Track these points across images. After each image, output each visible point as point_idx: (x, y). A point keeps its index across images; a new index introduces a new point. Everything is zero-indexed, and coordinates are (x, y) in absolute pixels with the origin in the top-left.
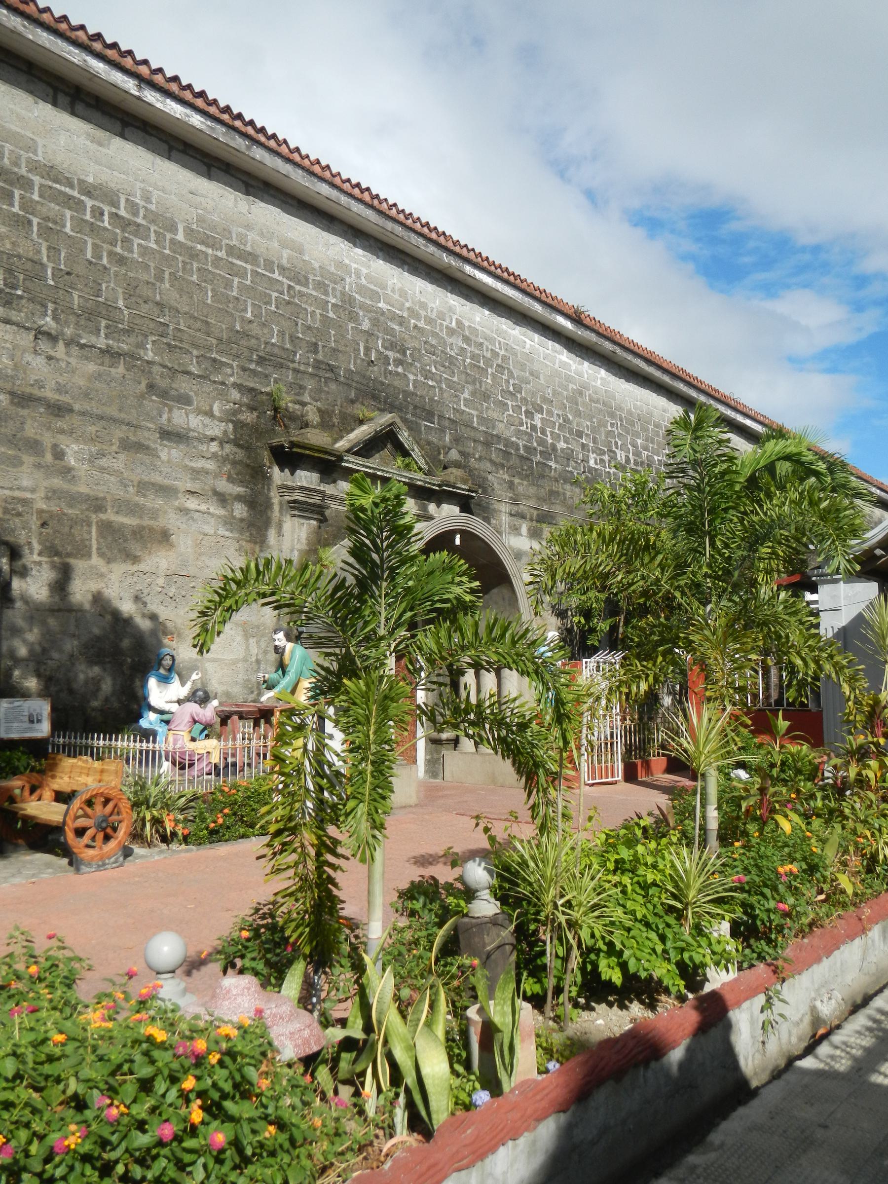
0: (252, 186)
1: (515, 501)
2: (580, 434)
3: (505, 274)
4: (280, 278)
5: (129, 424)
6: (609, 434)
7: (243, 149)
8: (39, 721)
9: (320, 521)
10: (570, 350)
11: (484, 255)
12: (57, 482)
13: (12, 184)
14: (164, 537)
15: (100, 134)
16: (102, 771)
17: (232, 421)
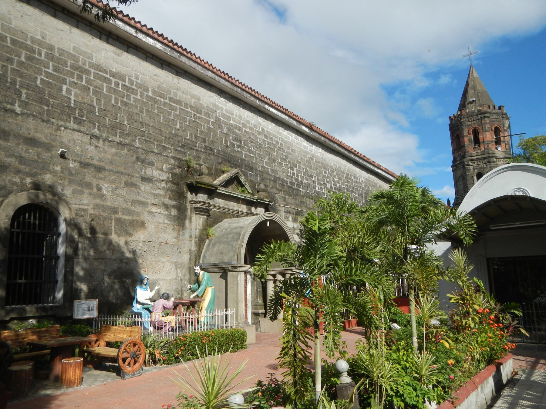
0: (180, 73)
1: (286, 206)
2: (312, 177)
3: (282, 109)
4: (191, 111)
5: (128, 175)
6: (324, 176)
7: (177, 57)
8: (92, 310)
9: (208, 216)
11: (273, 101)
12: (98, 201)
13: (82, 73)
14: (142, 225)
15: (119, 51)
17: (171, 173)
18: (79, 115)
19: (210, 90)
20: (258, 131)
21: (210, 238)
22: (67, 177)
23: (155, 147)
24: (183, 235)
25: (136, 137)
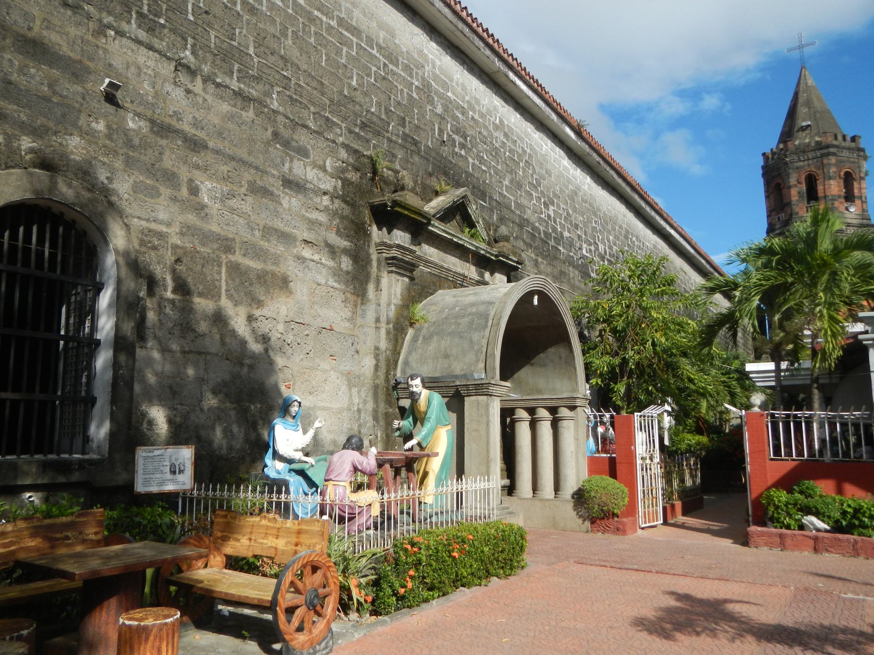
2: (576, 227)
3: (535, 84)
4: (378, 55)
5: (257, 168)
8: (181, 471)
9: (412, 279)
10: (569, 158)
11: (523, 66)
12: (191, 218)
14: (284, 283)
16: (299, 532)
18: (149, 11)
19: (412, 21)
21: (417, 325)
22: (121, 151)
23: (309, 116)
24: (363, 316)
25: (273, 86)
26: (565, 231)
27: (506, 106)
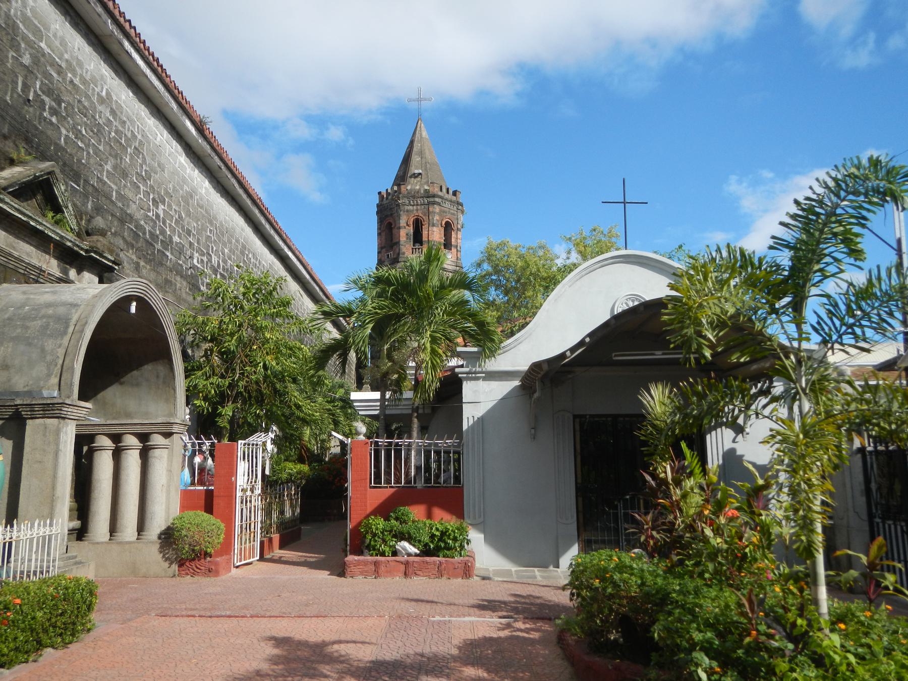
2: (189, 232)
10: (187, 155)
20: (98, 94)
26: (174, 235)
27: (117, 79)
